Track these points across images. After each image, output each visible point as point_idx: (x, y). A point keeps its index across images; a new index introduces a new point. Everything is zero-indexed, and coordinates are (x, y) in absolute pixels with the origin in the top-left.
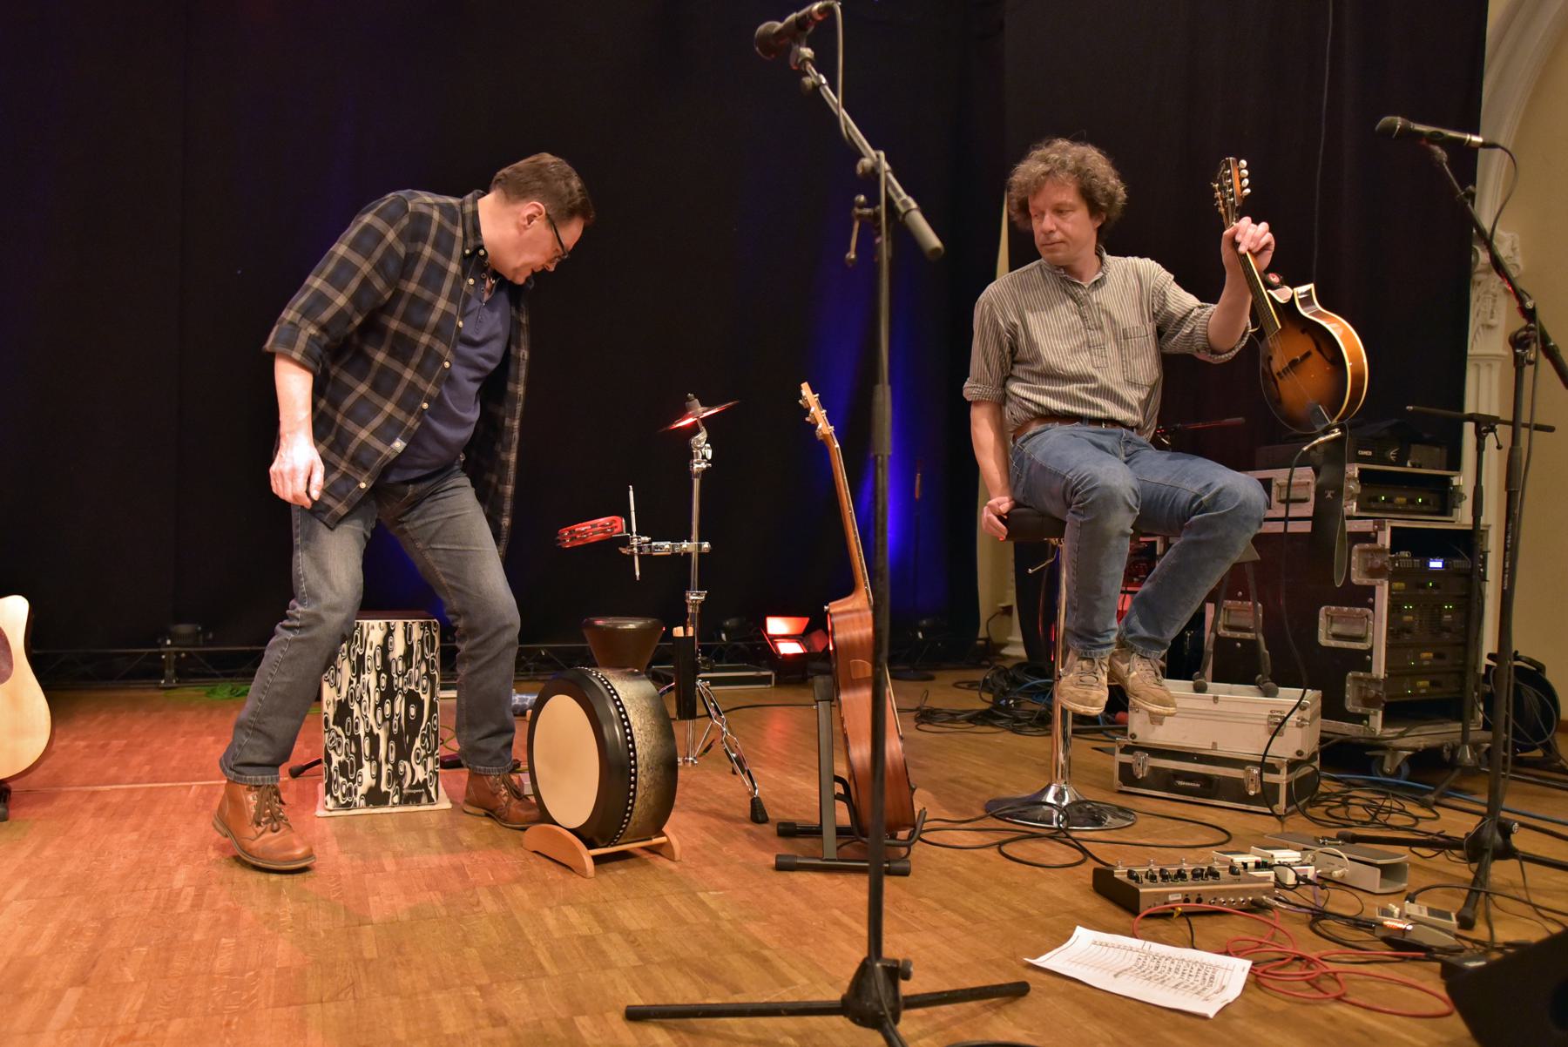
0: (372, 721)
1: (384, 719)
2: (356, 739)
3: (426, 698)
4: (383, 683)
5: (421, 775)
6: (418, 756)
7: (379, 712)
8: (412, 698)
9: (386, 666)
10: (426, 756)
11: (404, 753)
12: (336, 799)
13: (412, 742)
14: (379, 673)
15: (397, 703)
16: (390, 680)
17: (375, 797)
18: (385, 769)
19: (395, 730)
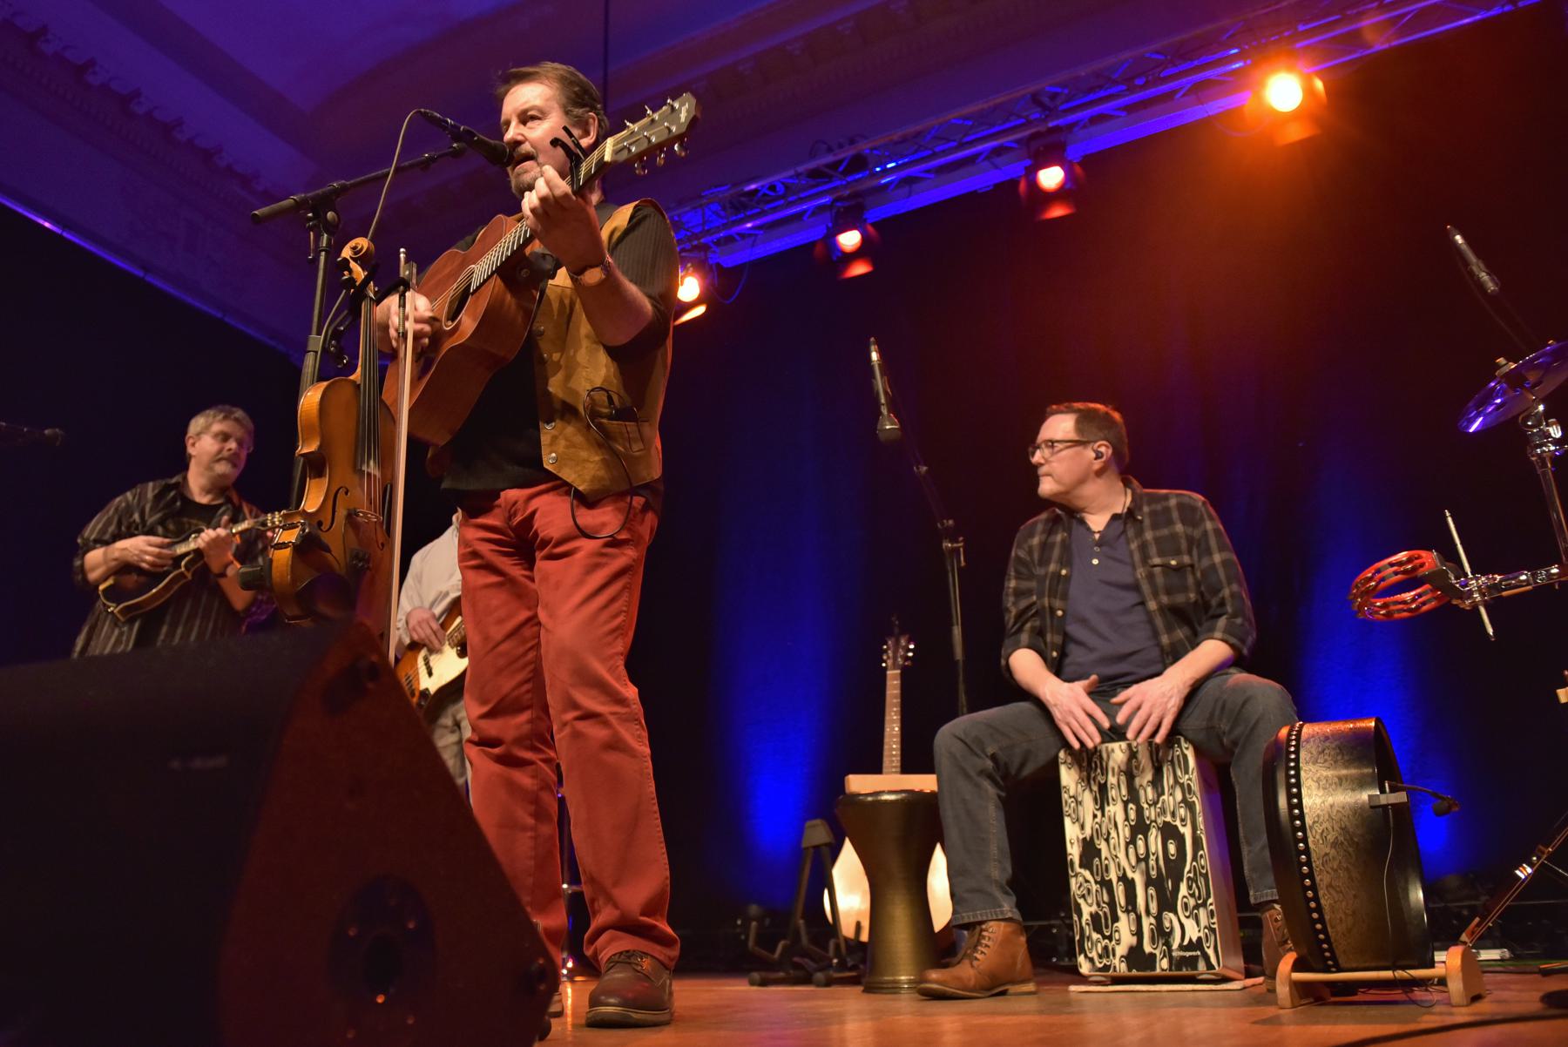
0: (1124, 863)
1: (1139, 860)
2: (1106, 884)
3: (1186, 831)
4: (1132, 815)
5: (1193, 932)
6: (1186, 906)
7: (1131, 851)
8: (1169, 832)
10: (1197, 907)
11: (1167, 903)
12: (1091, 960)
13: (1176, 889)
14: (1126, 804)
15: (1152, 839)
16: (1140, 811)
18: (1147, 923)
19: (1154, 873)
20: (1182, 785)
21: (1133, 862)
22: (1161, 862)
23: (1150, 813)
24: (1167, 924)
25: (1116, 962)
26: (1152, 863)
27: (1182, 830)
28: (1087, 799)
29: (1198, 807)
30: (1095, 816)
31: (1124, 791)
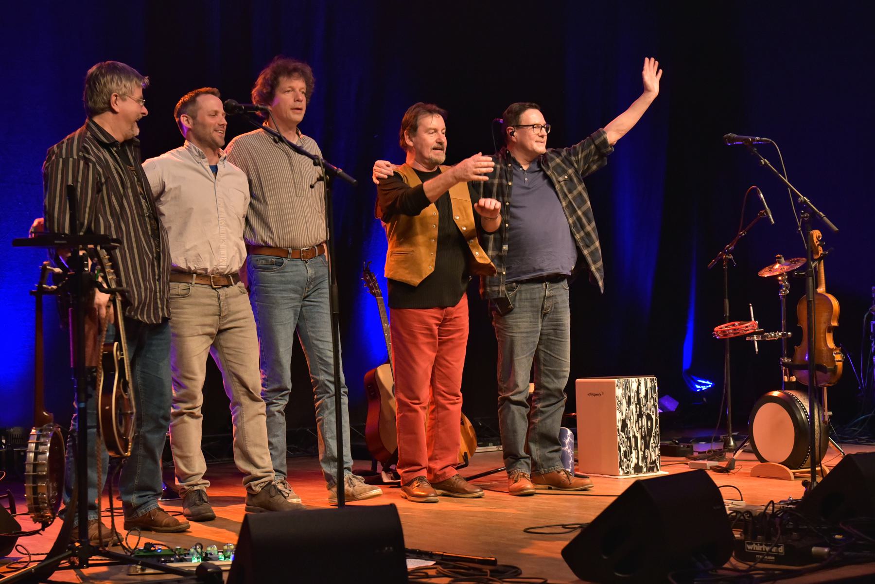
2: (629, 438)
3: (654, 417)
5: (654, 458)
8: (649, 417)
9: (639, 400)
11: (647, 446)
16: (640, 408)
23: (644, 409)
28: (624, 402)
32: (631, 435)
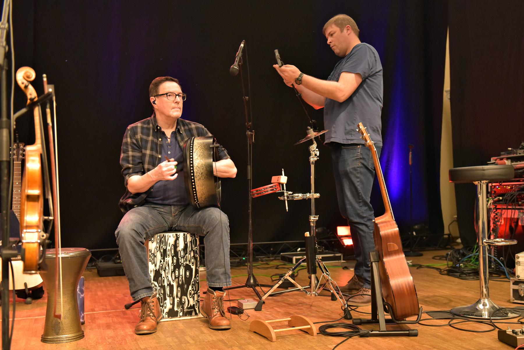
0: (170, 279)
1: (176, 278)
2: (163, 287)
3: (193, 267)
5: (192, 303)
7: (173, 274)
8: (188, 268)
9: (176, 254)
10: (194, 294)
11: (184, 293)
13: (188, 288)
14: (173, 257)
15: (181, 270)
16: (178, 260)
17: (172, 313)
19: (180, 282)
20: (194, 251)
21: (174, 278)
22: (184, 279)
23: (182, 261)
24: (183, 300)
25: (164, 314)
26: (180, 279)
27: (192, 267)
28: (159, 255)
29: (198, 259)
30: (161, 261)
31: (173, 252)
32: (166, 284)
